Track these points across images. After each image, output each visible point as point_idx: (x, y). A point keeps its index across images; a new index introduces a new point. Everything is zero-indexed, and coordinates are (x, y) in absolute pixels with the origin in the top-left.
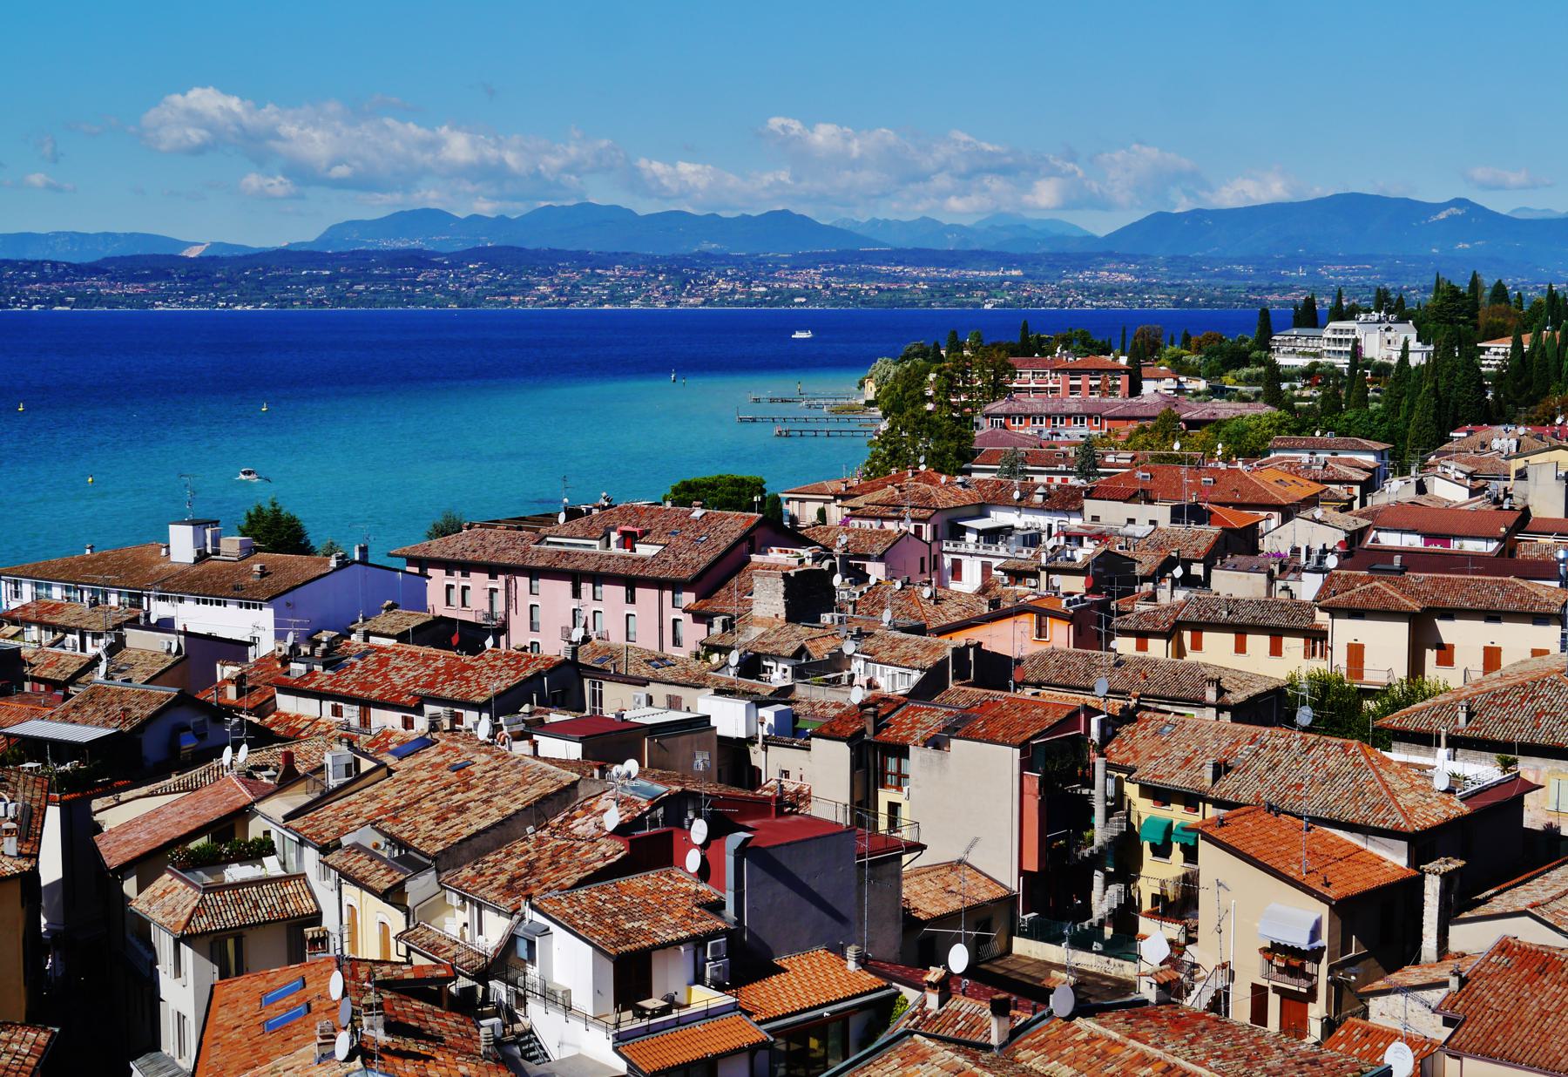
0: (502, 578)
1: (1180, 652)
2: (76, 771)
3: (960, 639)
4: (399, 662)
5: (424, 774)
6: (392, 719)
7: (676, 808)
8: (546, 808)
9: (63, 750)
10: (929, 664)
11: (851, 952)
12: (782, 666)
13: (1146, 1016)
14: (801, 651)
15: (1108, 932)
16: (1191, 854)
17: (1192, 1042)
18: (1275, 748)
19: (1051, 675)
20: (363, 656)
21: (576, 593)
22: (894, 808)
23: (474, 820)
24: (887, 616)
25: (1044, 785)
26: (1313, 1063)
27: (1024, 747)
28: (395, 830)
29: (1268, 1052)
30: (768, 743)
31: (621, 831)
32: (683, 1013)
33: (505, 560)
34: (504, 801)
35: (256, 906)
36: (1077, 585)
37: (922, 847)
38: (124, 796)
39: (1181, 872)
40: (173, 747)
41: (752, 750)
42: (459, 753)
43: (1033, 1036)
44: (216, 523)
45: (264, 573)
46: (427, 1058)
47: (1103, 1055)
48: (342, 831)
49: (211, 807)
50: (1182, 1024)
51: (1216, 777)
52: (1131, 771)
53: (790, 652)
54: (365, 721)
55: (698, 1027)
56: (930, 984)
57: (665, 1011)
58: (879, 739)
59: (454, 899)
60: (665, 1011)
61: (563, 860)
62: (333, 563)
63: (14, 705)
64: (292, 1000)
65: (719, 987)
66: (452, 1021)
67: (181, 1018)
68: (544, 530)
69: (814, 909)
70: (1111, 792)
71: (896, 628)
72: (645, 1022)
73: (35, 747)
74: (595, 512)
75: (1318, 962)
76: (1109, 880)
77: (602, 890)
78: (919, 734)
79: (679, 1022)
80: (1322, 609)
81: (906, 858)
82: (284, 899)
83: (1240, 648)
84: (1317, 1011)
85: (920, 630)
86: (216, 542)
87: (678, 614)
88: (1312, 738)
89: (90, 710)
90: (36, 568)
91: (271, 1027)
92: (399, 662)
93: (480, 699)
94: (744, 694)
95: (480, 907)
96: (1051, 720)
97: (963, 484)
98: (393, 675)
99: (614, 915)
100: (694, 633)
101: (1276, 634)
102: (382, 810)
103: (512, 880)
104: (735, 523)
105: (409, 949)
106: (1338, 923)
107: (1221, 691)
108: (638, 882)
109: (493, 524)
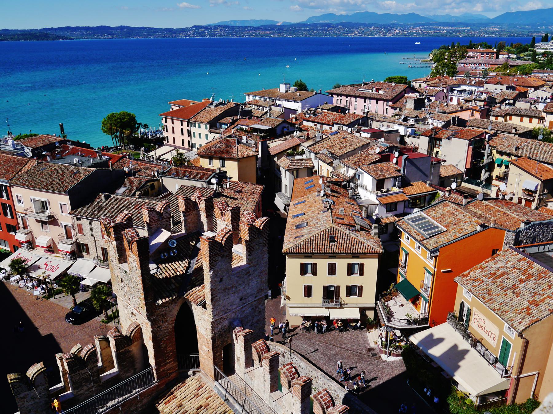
0: (349, 98)
1: (506, 121)
2: (264, 135)
3: (454, 115)
4: (329, 115)
5: (337, 139)
6: (327, 127)
7: (391, 149)
8: (363, 148)
9: (261, 131)
10: (446, 121)
11: (428, 182)
12: (412, 119)
13: (499, 202)
14: (417, 116)
15: (484, 183)
16: (507, 167)
17: (510, 208)
18: (532, 144)
19: (475, 124)
20: (321, 114)
21: (365, 102)
22: (437, 152)
23: (348, 149)
24: (437, 109)
25: (474, 149)
26: (539, 215)
27: (470, 140)
28: (331, 150)
29: (528, 212)
30: (409, 136)
31: (379, 153)
32: (391, 192)
33: (350, 94)
34: (354, 146)
35: (301, 164)
36: (482, 104)
37: (446, 161)
38: (274, 141)
39: (504, 171)
40: (283, 131)
41: (405, 137)
42: (344, 135)
43: (472, 203)
44: (290, 84)
45: (299, 95)
46: (338, 197)
47: (489, 209)
48: (320, 150)
49: (292, 144)
50: (507, 204)
51: (516, 150)
52: (495, 147)
53: (414, 117)
54: (321, 127)
55: (394, 195)
56: (447, 191)
57: (387, 192)
58: (435, 137)
59: (343, 165)
60: (387, 192)
61: (366, 159)
62: (314, 93)
63: (251, 121)
64: (310, 184)
65: (399, 187)
66: (343, 190)
67: (286, 186)
68: (359, 87)
69: (420, 173)
70: (489, 152)
71: (439, 112)
72: (383, 194)
73: (255, 130)
74: (370, 83)
75: (536, 194)
76: (486, 171)
77: (375, 166)
78: (445, 136)
79: (390, 194)
80: (544, 112)
81: (442, 163)
82: (307, 163)
83: (521, 120)
84: (534, 205)
85: (445, 113)
86: (289, 88)
87: (388, 107)
88: (541, 142)
89: (266, 123)
90: (253, 93)
91: (307, 189)
92: (329, 115)
93: (346, 124)
94: (404, 125)
95: (348, 167)
96: (477, 135)
97: (455, 79)
98: (327, 118)
99: (377, 171)
100: (391, 112)
101: (531, 117)
102: (328, 146)
103: (355, 162)
104: (402, 87)
105: (333, 175)
106: (543, 185)
107: (516, 130)
108: (382, 164)
109: (347, 86)
